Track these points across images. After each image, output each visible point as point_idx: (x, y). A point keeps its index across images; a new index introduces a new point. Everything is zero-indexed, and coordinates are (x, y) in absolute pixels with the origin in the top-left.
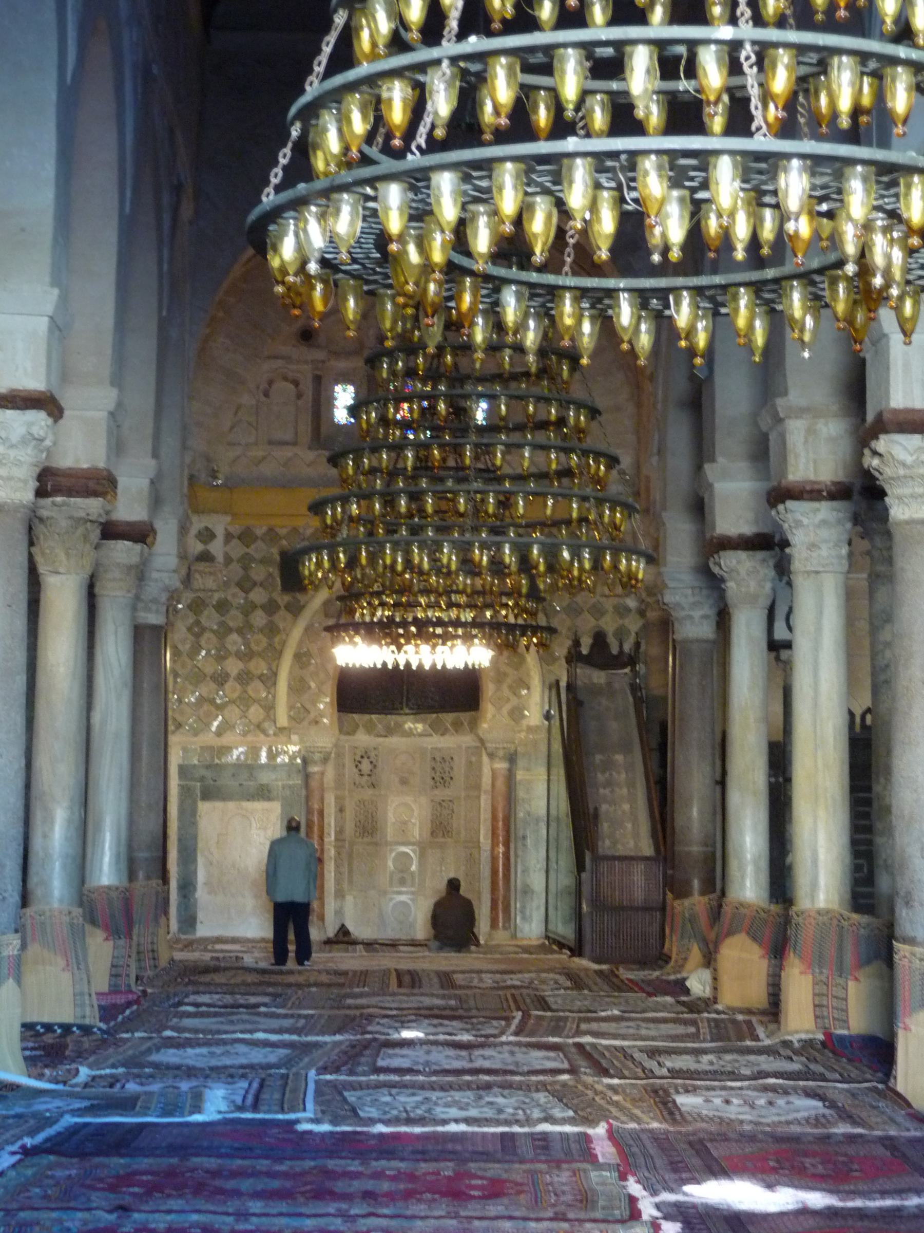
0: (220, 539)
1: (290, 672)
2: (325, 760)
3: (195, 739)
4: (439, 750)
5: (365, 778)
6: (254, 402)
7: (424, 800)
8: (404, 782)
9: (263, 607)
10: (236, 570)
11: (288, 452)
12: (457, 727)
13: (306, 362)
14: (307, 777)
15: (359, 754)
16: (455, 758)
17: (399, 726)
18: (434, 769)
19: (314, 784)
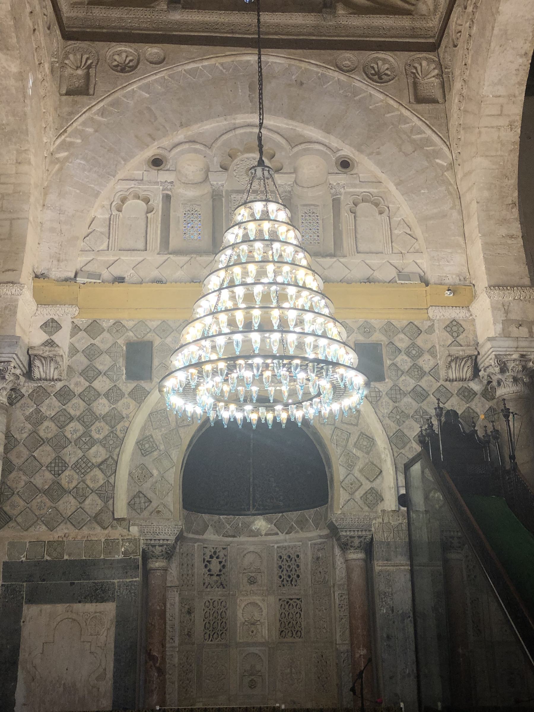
0: (66, 328)
1: (132, 460)
2: (169, 555)
3: (25, 533)
4: (285, 548)
5: (215, 578)
6: (107, 216)
7: (272, 599)
8: (252, 581)
9: (107, 395)
10: (81, 360)
11: (138, 257)
12: (302, 524)
13: (157, 183)
14: (147, 573)
15: (208, 554)
16: (301, 556)
17: (247, 526)
18: (280, 567)
19: (155, 581)
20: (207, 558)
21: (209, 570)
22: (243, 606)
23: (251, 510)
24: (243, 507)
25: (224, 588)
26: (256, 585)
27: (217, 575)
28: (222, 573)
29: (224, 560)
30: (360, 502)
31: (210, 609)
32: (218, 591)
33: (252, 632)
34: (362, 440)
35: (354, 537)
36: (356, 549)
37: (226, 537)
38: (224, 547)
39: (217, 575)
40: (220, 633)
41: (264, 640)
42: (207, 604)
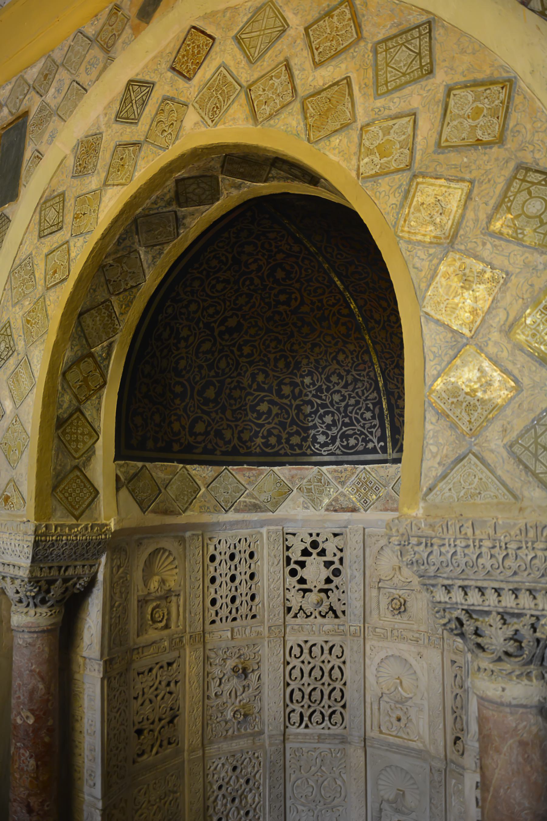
15: (298, 547)
20: (296, 555)
21: (302, 581)
22: (377, 660)
23: (390, 450)
24: (370, 445)
25: (336, 617)
26: (405, 616)
27: (321, 591)
28: (332, 586)
29: (336, 559)
30: (507, 469)
31: (303, 662)
32: (323, 625)
33: (399, 720)
34: (524, 195)
35: (488, 613)
36: (500, 659)
37: (336, 511)
38: (337, 531)
39: (321, 591)
40: (327, 713)
41: (420, 745)
42: (296, 651)
